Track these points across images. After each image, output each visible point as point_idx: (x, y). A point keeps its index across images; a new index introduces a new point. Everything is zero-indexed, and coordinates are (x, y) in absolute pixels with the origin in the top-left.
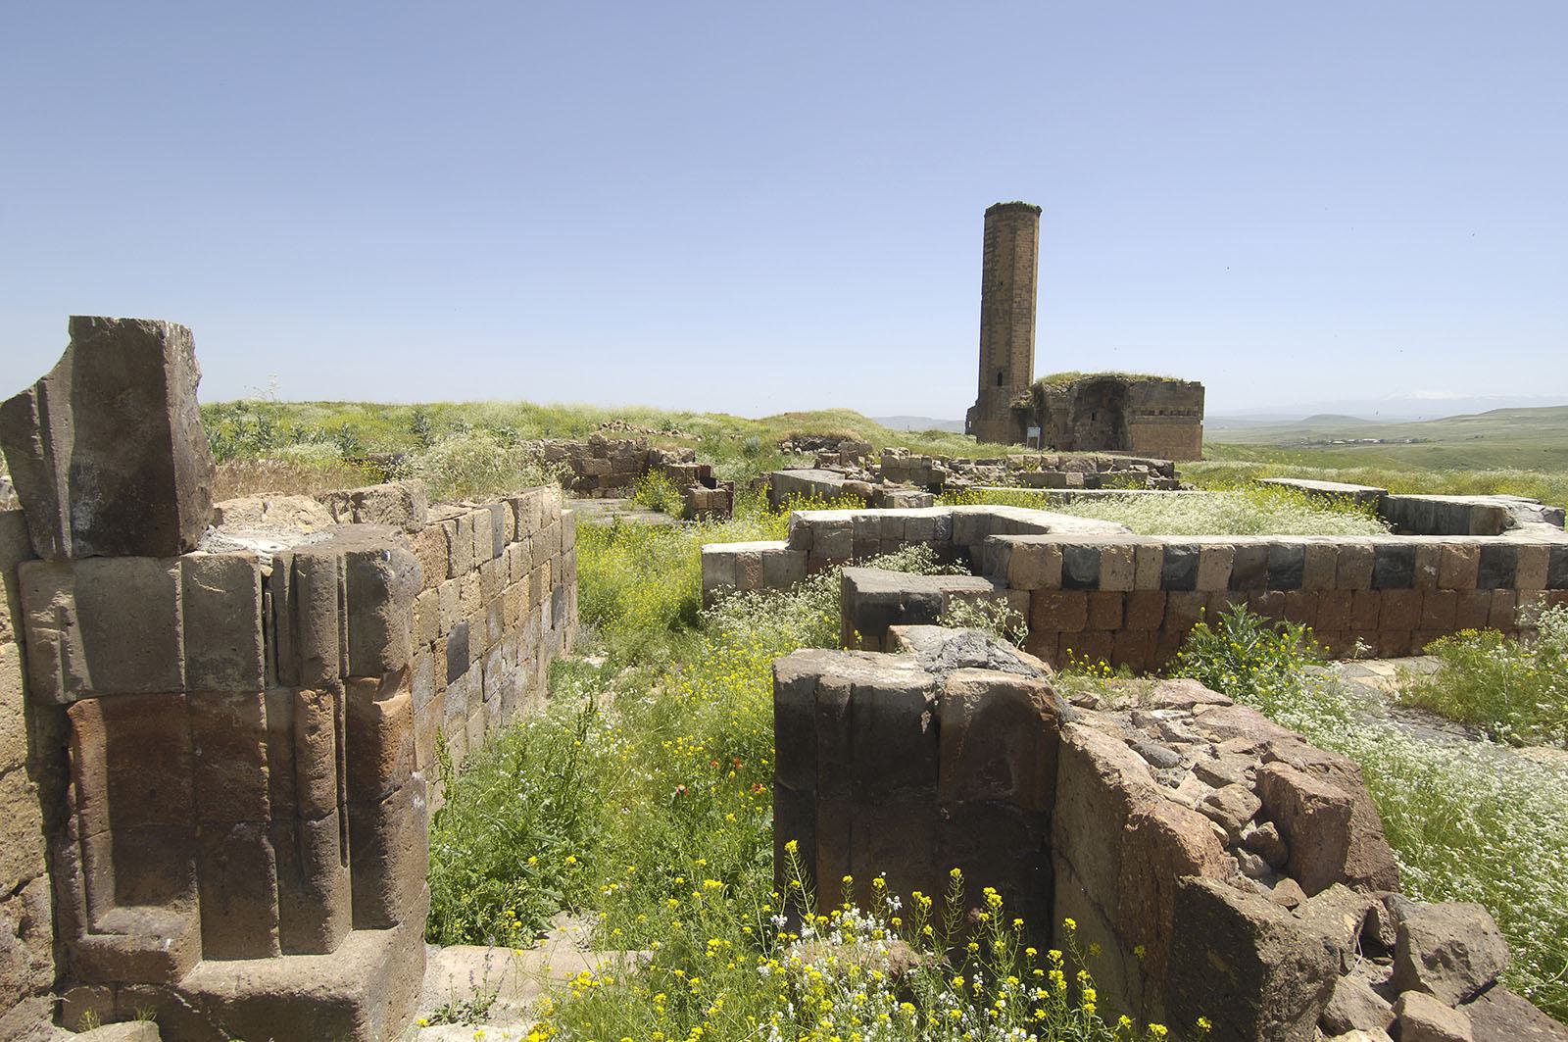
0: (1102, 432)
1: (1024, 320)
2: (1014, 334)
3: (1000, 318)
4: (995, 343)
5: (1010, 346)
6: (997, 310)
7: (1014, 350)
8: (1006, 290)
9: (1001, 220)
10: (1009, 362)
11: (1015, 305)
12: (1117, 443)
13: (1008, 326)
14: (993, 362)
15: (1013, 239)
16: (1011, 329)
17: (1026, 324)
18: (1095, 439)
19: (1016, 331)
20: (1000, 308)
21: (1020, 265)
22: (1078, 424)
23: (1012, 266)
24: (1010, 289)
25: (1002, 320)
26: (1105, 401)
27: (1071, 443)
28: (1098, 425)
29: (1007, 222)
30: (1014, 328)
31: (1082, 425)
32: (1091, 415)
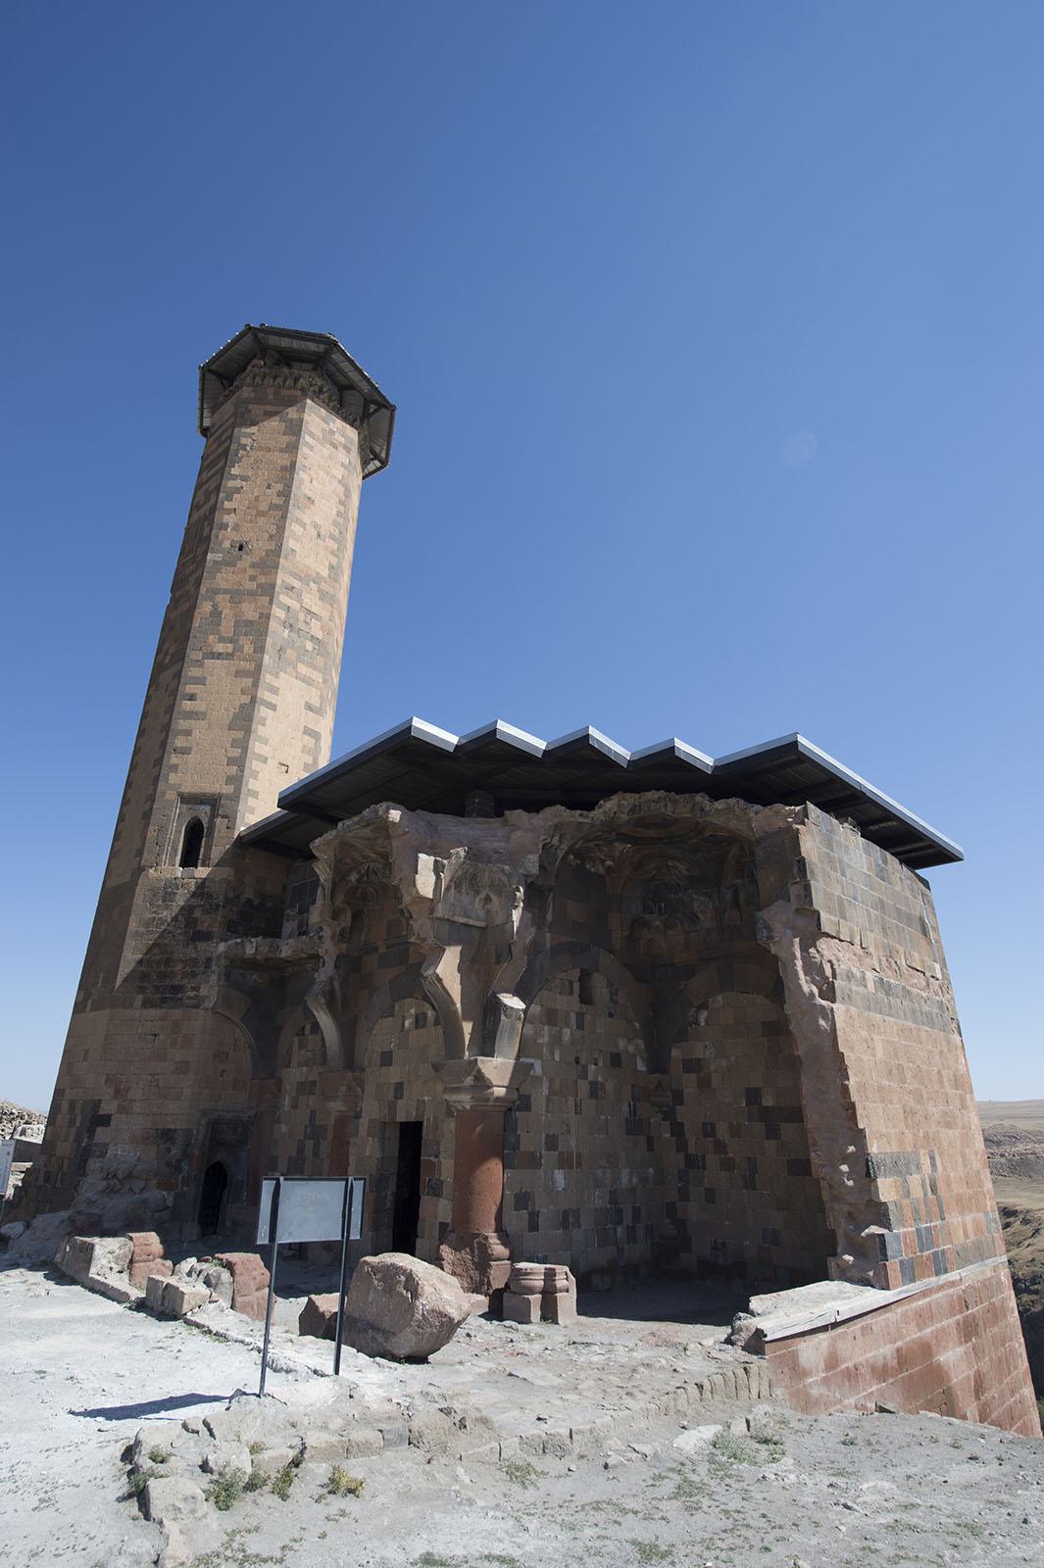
0: (616, 1060)
1: (303, 669)
2: (264, 694)
3: (222, 640)
4: (192, 715)
5: (248, 731)
6: (216, 614)
7: (256, 747)
8: (253, 566)
10: (237, 781)
11: (278, 612)
13: (244, 665)
14: (173, 778)
15: (293, 448)
16: (256, 674)
18: (595, 1090)
19: (275, 691)
20: (227, 612)
25: (230, 647)
30: (267, 678)
32: (577, 973)
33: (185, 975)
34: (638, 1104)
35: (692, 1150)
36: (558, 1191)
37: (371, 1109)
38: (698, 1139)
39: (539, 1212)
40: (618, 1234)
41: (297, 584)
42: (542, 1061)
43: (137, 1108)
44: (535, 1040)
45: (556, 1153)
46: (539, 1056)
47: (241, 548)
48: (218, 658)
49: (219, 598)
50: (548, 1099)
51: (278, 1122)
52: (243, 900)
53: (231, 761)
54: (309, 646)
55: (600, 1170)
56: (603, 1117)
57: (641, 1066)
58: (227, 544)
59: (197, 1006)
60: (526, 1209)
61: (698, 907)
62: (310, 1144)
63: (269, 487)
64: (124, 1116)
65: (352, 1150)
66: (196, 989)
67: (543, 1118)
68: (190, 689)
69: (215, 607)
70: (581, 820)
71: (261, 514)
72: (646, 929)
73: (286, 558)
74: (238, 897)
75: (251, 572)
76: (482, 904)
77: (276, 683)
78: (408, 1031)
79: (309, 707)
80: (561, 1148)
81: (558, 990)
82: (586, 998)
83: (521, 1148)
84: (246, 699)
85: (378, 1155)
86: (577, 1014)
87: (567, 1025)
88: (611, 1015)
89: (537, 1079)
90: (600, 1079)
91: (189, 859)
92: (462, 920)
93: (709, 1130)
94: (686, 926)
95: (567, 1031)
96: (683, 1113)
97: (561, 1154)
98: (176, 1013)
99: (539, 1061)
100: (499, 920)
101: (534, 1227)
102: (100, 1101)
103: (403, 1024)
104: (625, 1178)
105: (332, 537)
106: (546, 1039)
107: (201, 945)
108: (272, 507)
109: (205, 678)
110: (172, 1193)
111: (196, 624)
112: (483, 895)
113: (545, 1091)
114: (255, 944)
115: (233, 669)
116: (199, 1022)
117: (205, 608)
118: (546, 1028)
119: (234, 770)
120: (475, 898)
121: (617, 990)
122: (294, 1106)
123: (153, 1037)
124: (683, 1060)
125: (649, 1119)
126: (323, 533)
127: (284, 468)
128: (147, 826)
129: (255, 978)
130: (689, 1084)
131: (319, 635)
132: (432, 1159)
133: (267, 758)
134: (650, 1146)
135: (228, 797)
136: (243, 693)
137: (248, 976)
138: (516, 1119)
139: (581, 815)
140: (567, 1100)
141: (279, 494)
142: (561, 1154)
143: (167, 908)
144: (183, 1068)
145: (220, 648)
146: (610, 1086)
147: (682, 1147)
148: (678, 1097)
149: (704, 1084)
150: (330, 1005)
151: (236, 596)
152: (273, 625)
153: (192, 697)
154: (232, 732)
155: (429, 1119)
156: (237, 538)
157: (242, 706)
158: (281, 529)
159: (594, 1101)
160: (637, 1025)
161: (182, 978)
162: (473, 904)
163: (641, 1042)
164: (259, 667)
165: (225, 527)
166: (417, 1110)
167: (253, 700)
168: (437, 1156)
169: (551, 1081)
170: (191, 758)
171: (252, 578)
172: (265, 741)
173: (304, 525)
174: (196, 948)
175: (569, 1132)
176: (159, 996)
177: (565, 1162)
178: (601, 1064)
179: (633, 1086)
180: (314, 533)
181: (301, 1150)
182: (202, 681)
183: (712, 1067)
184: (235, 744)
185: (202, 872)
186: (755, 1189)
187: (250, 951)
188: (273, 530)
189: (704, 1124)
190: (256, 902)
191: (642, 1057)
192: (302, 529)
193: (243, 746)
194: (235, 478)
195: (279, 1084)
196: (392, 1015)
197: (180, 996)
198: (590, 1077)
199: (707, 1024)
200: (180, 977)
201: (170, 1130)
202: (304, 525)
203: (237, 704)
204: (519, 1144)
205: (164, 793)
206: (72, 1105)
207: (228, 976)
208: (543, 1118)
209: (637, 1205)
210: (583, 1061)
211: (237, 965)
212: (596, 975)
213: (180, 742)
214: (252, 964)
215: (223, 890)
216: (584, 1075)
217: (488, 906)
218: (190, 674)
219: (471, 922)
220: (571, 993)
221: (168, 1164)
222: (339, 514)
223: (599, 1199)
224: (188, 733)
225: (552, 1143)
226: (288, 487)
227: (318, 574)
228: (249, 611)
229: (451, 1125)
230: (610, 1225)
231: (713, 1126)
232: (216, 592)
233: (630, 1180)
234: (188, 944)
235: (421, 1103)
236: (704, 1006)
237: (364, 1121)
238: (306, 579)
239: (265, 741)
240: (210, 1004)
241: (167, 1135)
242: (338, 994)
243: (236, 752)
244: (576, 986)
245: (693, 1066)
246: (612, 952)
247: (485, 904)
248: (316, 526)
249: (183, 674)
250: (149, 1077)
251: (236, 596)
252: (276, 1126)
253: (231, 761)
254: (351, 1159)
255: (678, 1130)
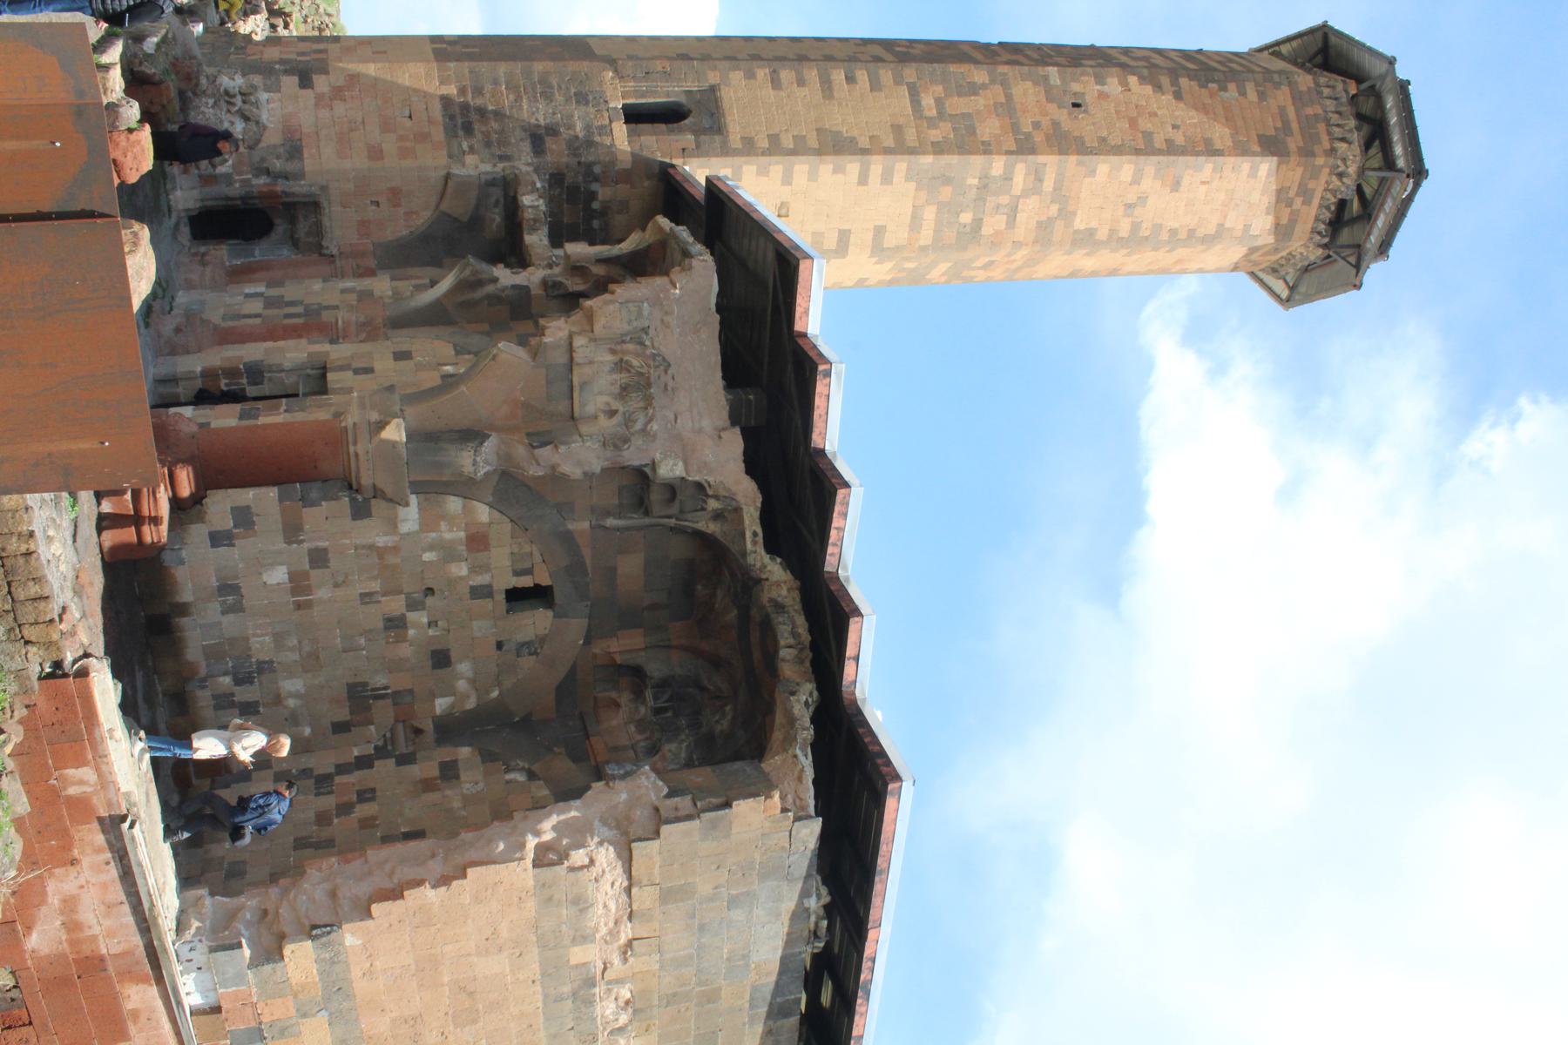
0: (441, 659)
1: (930, 214)
2: (877, 164)
3: (939, 102)
5: (819, 152)
6: (974, 90)
7: (801, 167)
8: (1056, 124)
9: (1298, 98)
11: (998, 165)
12: (382, 752)
13: (911, 136)
14: (737, 77)
16: (901, 148)
17: (915, 223)
18: (395, 624)
19: (887, 178)
20: (979, 102)
21: (1147, 183)
22: (483, 513)
23: (1145, 147)
24: (1063, 143)
26: (625, 645)
27: (351, 487)
28: (483, 629)
29: (1295, 126)
30: (901, 165)
31: (478, 541)
32: (545, 580)
33: (486, 135)
34: (389, 701)
35: (338, 779)
36: (261, 574)
37: (338, 352)
38: (353, 784)
39: (233, 545)
40: (221, 679)
41: (1048, 185)
42: (417, 532)
43: (324, 114)
44: (443, 517)
45: (307, 567)
46: (426, 524)
47: (1076, 105)
48: (912, 101)
49: (998, 89)
50: (372, 547)
51: (325, 281)
52: (595, 187)
53: (774, 139)
54: (966, 218)
55: (296, 642)
56: (362, 641)
57: (441, 704)
58: (1076, 87)
59: (450, 156)
60: (235, 526)
61: (670, 751)
62: (300, 309)
63: (1174, 127)
64: (313, 101)
65: (291, 343)
66: (472, 150)
67: (348, 542)
68: (862, 76)
69: (984, 86)
70: (748, 535)
71: (1133, 123)
72: (632, 696)
73: (1079, 164)
74: (596, 179)
75: (1045, 122)
76: (602, 408)
77: (898, 177)
78: (439, 370)
79: (879, 231)
80: (314, 573)
81: (516, 550)
82: (516, 597)
83: (304, 510)
84: (864, 142)
85: (287, 365)
86: (490, 586)
87: (475, 569)
88: (499, 645)
89: (392, 524)
90: (411, 632)
91: (635, 116)
92: (576, 382)
93: (366, 795)
94: (642, 744)
95: (461, 570)
96: (386, 767)
97: (306, 575)
98: (438, 134)
99: (416, 527)
100: (584, 429)
101: (217, 539)
102: (327, 73)
103: (446, 365)
104: (292, 685)
105: (1135, 227)
106: (448, 536)
107: (526, 147)
108: (1148, 136)
109: (880, 90)
110: (231, 171)
111: (952, 68)
112: (616, 405)
113: (382, 541)
114: (536, 204)
115: (901, 121)
116: (433, 161)
117: (980, 75)
118: (462, 534)
119: (764, 143)
120: (609, 395)
121: (535, 653)
122: (343, 291)
123: (407, 114)
124: (455, 762)
125: (372, 724)
126: (1138, 211)
127: (1208, 142)
128: (669, 59)
129: (496, 218)
130: (427, 768)
131: (987, 230)
132: (284, 407)
133: (790, 184)
134: (340, 728)
135: (725, 143)
136: (871, 138)
137: (497, 210)
138: (337, 498)
139: (755, 534)
140: (374, 578)
141: (1169, 142)
142: (306, 575)
143: (568, 100)
144: (376, 153)
145: (928, 101)
146: (405, 651)
147: (342, 769)
148: (405, 760)
149: (427, 785)
150: (462, 286)
151: (1007, 108)
152: (978, 161)
153: (850, 79)
154: (815, 133)
155: (330, 399)
156: (1089, 99)
157: (853, 140)
158: (1118, 150)
159: (381, 625)
160: (495, 694)
161: (482, 132)
162: (600, 393)
163: (471, 704)
164: (912, 151)
165: (1100, 80)
166: (342, 389)
167: (865, 152)
168: (285, 411)
169: (395, 549)
170: (770, 92)
171: (1036, 125)
172: (813, 176)
173: (1136, 181)
174: (522, 140)
175: (336, 585)
176: (458, 111)
177: (298, 583)
178: (431, 632)
179: (411, 691)
180: (1131, 198)
181: (292, 304)
182: (875, 86)
183: (448, 792)
184: (800, 140)
185: (620, 130)
186: (295, 848)
187: (527, 200)
188: (1114, 140)
189: (373, 790)
190: (596, 205)
191: (452, 706)
192: (1129, 179)
193: (799, 149)
194: (1175, 83)
195: (370, 273)
196: (458, 353)
197: (461, 133)
198: (412, 616)
199: (508, 782)
200: (484, 129)
201: (302, 155)
202: (1136, 181)
203: (855, 133)
204: (311, 506)
205: (714, 69)
206: (325, 51)
207: (492, 183)
208: (348, 542)
209: (261, 710)
210: (430, 601)
211: (508, 189)
212: (550, 613)
213: (786, 75)
214: (512, 209)
215: (602, 158)
216: (413, 605)
217: (602, 416)
218: (882, 72)
219: (576, 395)
220: (517, 573)
221: (263, 159)
222: (1173, 232)
223: (261, 645)
224: (801, 82)
225: (319, 558)
226: (1183, 151)
227: (1074, 214)
228: (989, 128)
229: (323, 415)
230: (230, 664)
231: (373, 799)
232: (1004, 84)
233: (291, 695)
234: (525, 131)
235: (350, 390)
236: (532, 776)
237: (327, 347)
238: (1060, 195)
239: (813, 176)
240: (457, 170)
241: (294, 150)
242: (479, 294)
243: (787, 142)
244: (526, 582)
245: (449, 772)
246: (588, 641)
247: (604, 412)
248: (1142, 200)
249: (880, 64)
250: (360, 119)
251: (1007, 108)
252: (321, 280)
253: (774, 139)
254: (281, 343)
255: (364, 763)
